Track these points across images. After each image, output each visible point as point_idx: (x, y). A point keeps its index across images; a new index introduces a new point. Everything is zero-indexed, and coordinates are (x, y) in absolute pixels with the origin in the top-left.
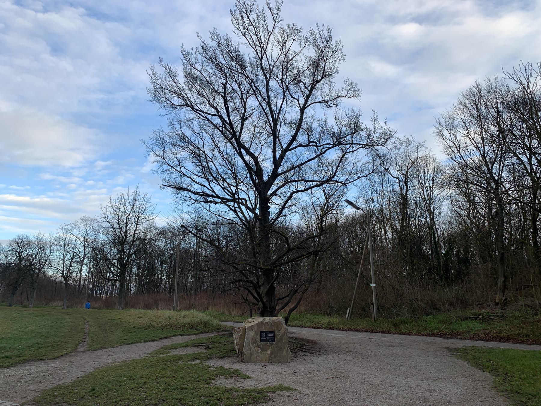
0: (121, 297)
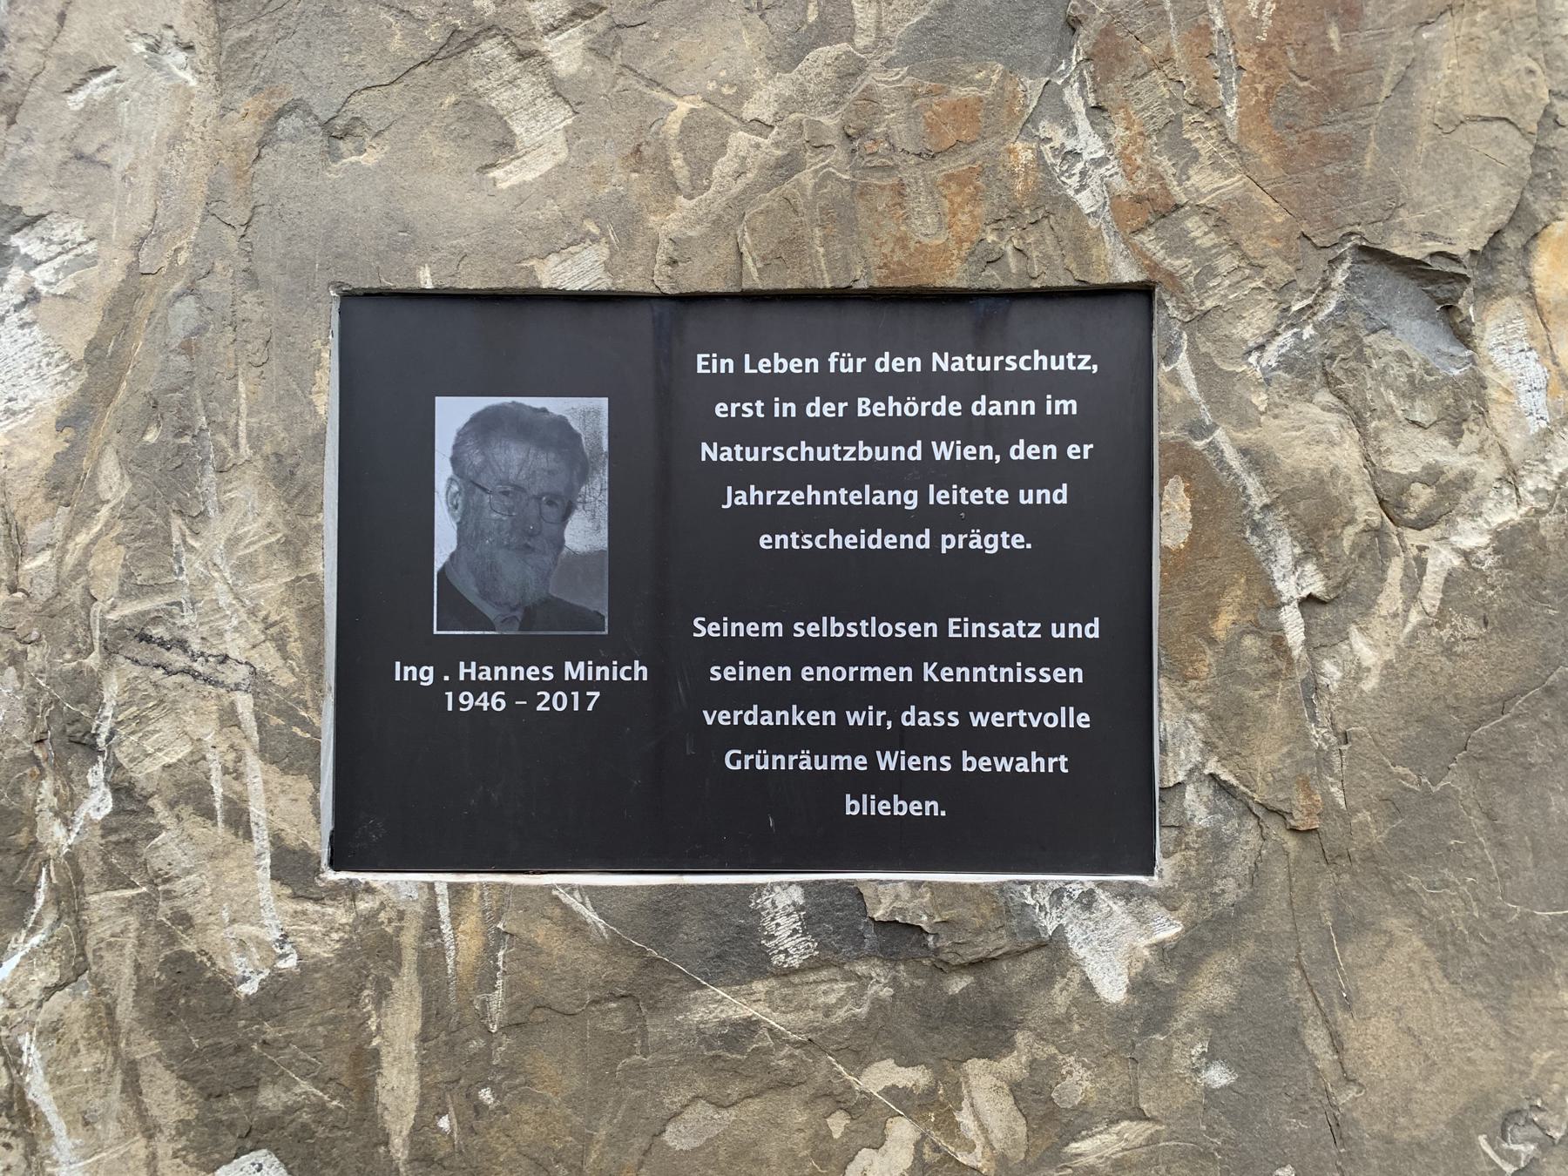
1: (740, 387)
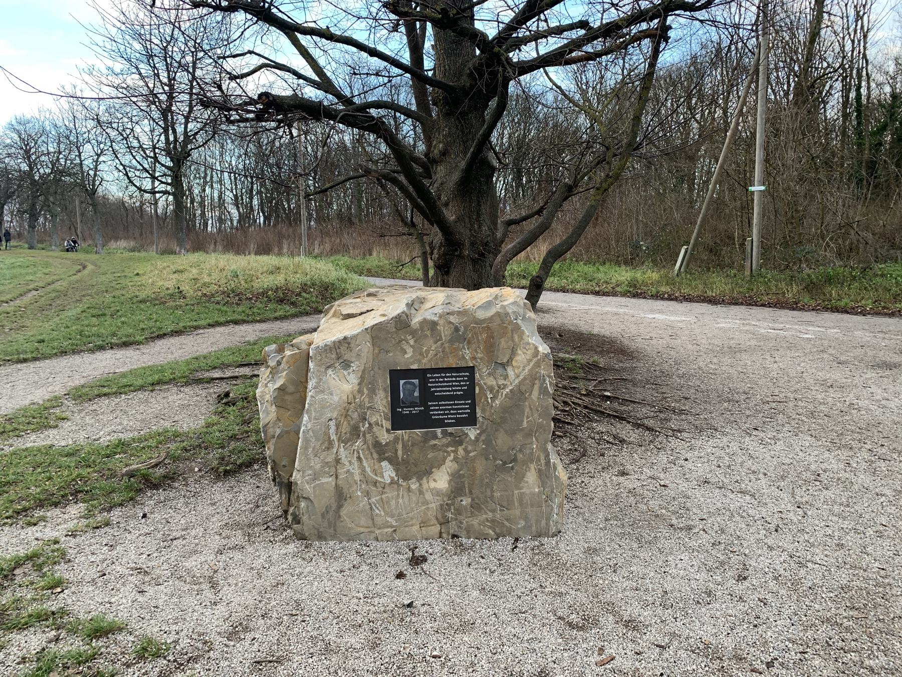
0: (182, 229)
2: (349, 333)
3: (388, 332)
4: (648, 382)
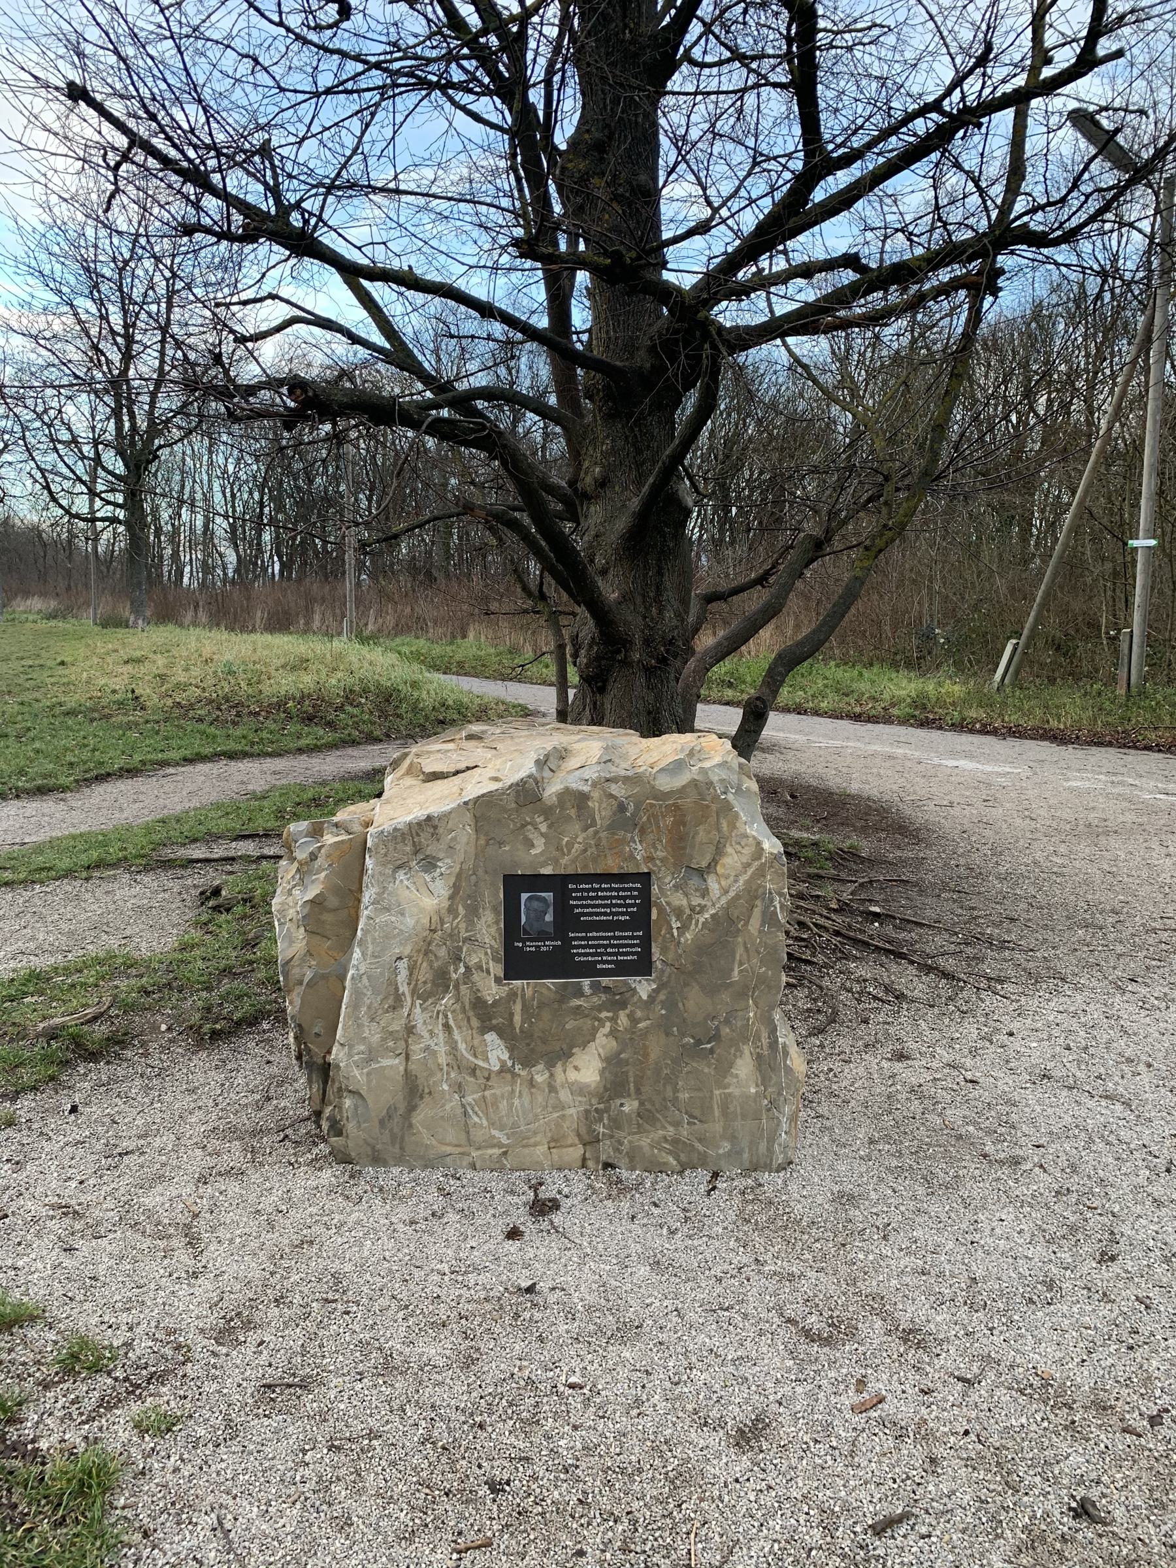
1: (577, 890)
2: (435, 809)
3: (505, 810)
4: (945, 887)
